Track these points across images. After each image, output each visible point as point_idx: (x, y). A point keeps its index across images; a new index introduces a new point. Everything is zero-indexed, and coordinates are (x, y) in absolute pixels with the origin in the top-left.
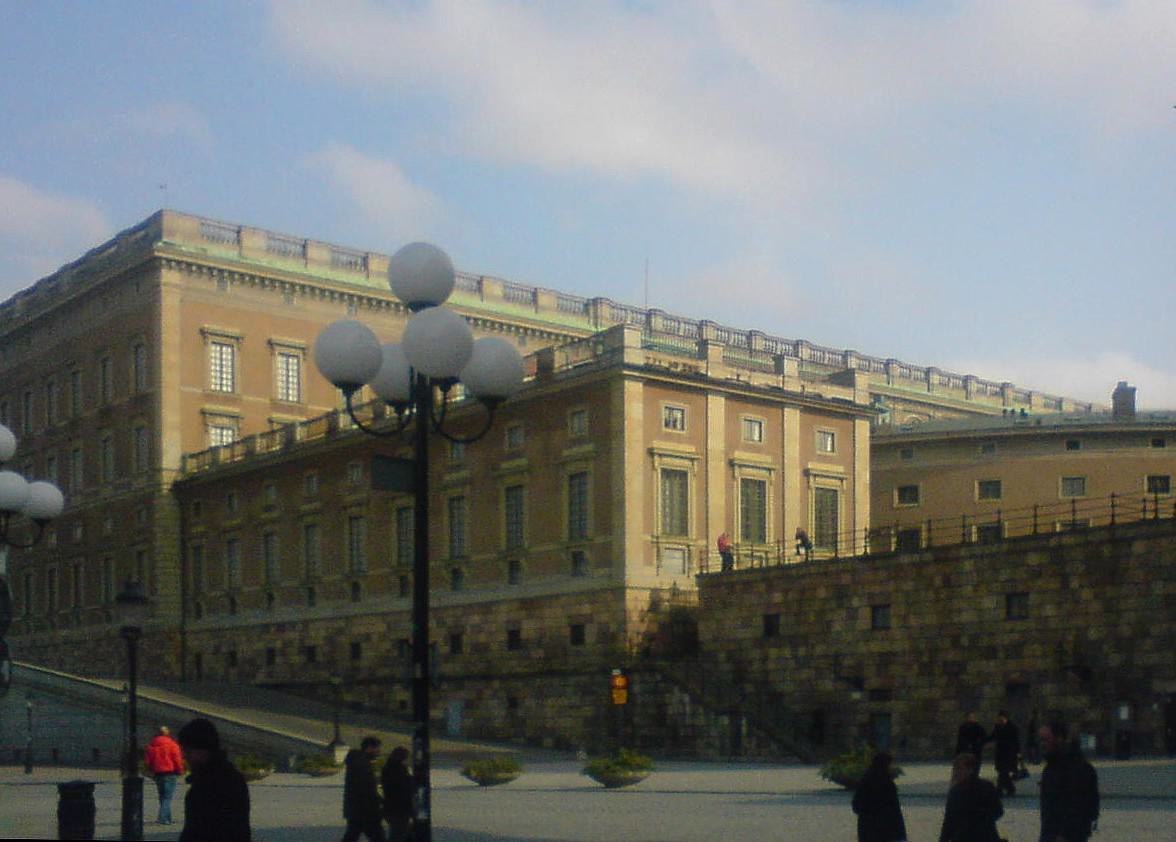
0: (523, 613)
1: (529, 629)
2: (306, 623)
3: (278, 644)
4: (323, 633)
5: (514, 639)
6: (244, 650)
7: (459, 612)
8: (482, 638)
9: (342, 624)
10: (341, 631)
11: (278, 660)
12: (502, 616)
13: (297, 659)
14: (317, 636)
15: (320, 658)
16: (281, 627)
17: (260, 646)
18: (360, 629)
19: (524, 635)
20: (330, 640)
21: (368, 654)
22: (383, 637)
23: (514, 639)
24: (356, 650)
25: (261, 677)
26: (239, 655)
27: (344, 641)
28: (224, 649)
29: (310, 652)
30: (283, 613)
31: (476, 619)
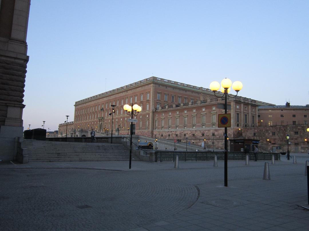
0: (215, 131)
1: (216, 133)
2: (176, 131)
3: (171, 134)
4: (179, 133)
5: (213, 135)
6: (164, 134)
7: (204, 131)
8: (208, 134)
9: (183, 131)
10: (182, 132)
11: (171, 136)
12: (212, 131)
13: (174, 136)
14: (178, 133)
15: (178, 136)
16: (171, 132)
17: (168, 134)
18: (186, 132)
19: (215, 134)
20: (180, 134)
21: (187, 136)
22: (190, 134)
23: (213, 135)
24: (185, 135)
25: (167, 138)
26: (163, 135)
27: (183, 134)
28: (161, 134)
29: (177, 135)
30: (173, 130)
31: (207, 132)
